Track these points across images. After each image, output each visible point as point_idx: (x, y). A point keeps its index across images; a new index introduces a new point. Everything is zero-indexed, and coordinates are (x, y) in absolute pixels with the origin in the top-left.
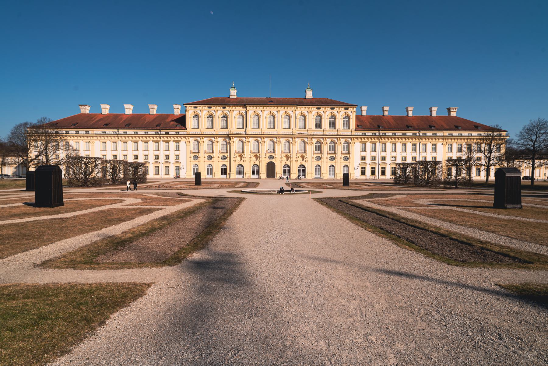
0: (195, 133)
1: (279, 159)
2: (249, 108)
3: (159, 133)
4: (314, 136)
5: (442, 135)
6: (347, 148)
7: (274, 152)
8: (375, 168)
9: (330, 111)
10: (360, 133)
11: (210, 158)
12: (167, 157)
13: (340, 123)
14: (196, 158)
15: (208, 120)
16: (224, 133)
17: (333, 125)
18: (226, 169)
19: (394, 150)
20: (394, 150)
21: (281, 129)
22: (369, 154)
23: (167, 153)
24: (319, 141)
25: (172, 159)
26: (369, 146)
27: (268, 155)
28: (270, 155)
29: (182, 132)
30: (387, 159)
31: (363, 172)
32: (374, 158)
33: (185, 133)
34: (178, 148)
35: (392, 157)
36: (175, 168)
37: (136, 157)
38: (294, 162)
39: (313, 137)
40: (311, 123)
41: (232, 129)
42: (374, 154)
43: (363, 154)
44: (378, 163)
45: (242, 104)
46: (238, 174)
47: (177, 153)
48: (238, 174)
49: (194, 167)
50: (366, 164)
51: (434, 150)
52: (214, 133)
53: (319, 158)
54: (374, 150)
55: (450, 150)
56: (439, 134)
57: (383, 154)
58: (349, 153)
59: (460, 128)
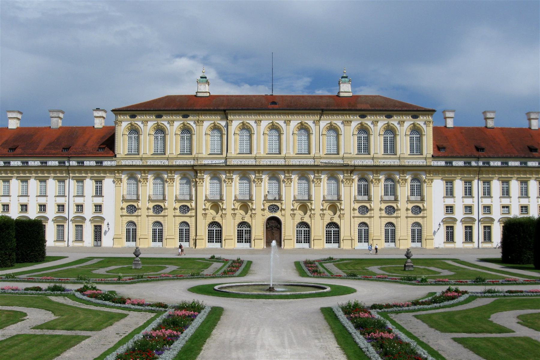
1: (288, 212)
7: (280, 200)
8: (471, 228)
9: (384, 120)
12: (80, 207)
14: (132, 209)
15: (156, 138)
18: (188, 231)
20: (506, 193)
21: (292, 154)
23: (79, 200)
25: (89, 212)
26: (459, 185)
27: (267, 205)
28: (271, 204)
31: (450, 237)
32: (469, 209)
33: (114, 163)
34: (99, 192)
35: (503, 207)
36: (93, 228)
37: (24, 207)
38: (318, 217)
41: (200, 156)
42: (468, 201)
43: (449, 201)
44: (477, 218)
46: (210, 240)
47: (98, 201)
48: (210, 240)
49: (128, 228)
50: (455, 220)
54: (468, 192)
57: (486, 201)
58: (422, 200)
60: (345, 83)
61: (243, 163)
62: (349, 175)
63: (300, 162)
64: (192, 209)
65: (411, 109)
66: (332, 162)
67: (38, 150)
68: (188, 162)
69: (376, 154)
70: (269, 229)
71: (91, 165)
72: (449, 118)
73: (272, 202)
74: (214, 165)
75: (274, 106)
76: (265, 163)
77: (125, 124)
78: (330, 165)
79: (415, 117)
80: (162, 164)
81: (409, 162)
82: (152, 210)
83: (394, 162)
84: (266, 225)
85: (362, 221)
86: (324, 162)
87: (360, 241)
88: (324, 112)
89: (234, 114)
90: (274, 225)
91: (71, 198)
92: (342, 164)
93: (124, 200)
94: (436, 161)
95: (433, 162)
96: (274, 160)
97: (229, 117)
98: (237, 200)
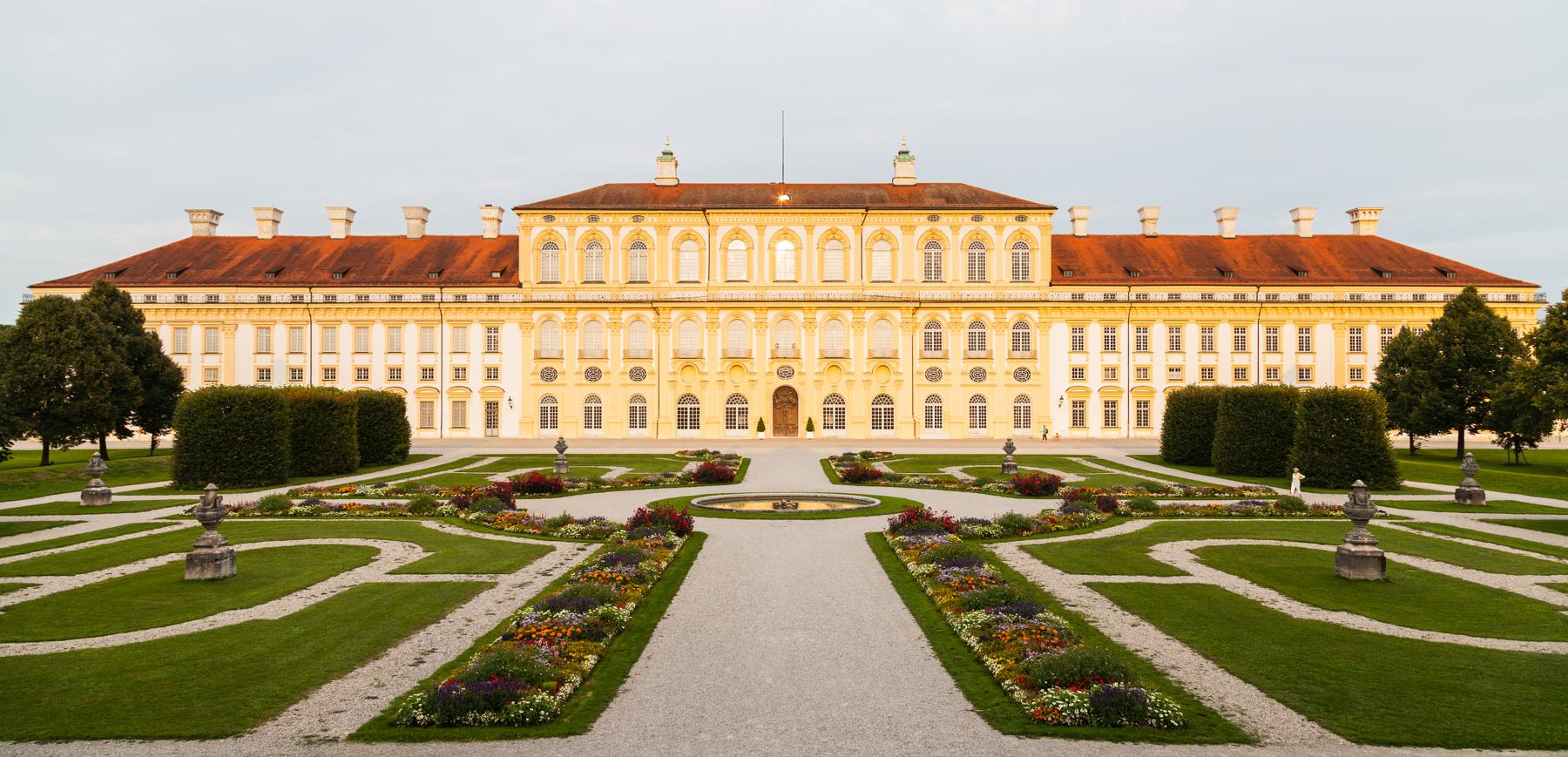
0: (547, 298)
2: (715, 217)
3: (437, 298)
4: (919, 304)
5: (1331, 298)
6: (1021, 341)
8: (1114, 404)
10: (1065, 292)
11: (593, 374)
12: (460, 373)
13: (999, 265)
14: (549, 375)
16: (638, 298)
17: (977, 270)
18: (643, 409)
19: (1176, 345)
20: (1176, 345)
22: (1094, 359)
23: (460, 360)
24: (938, 318)
25: (476, 379)
26: (1094, 336)
29: (506, 294)
30: (1122, 374)
31: (1078, 419)
32: (1111, 373)
34: (492, 346)
37: (363, 374)
39: (917, 308)
40: (913, 266)
41: (663, 285)
42: (1111, 359)
43: (1078, 360)
46: (682, 424)
47: (492, 360)
50: (1088, 391)
51: (1305, 346)
52: (608, 298)
53: (934, 375)
54: (1110, 344)
55: (1356, 345)
56: (1318, 293)
57: (1142, 359)
58: (1034, 358)
59: (1386, 275)
64: (653, 373)
65: (1016, 205)
67: (385, 277)
70: (779, 407)
77: (536, 231)
82: (584, 377)
84: (774, 400)
87: (928, 424)
88: (869, 212)
90: (785, 399)
91: (447, 357)
93: (538, 358)
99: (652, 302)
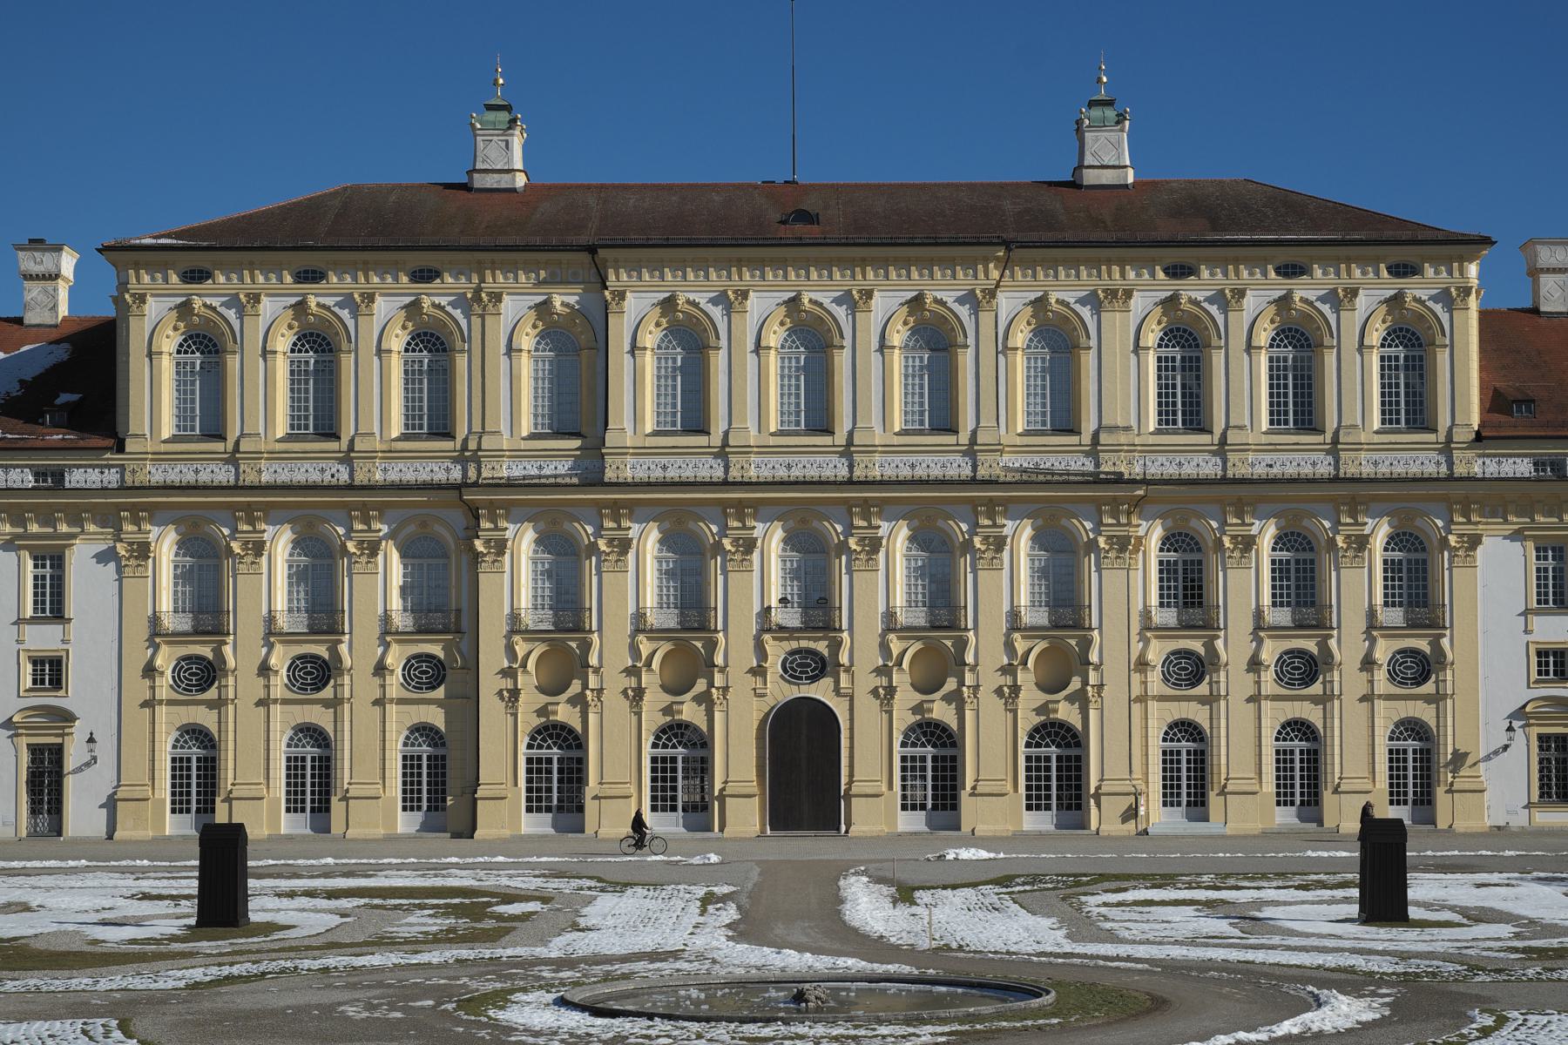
1: (866, 681)
28: (794, 645)
45: (572, 239)
47: (45, 638)
60: (1101, 125)
61: (672, 474)
62: (1123, 520)
63: (913, 466)
66: (1048, 465)
68: (436, 469)
69: (1236, 431)
71: (10, 484)
72: (1548, 271)
73: (798, 639)
74: (552, 480)
75: (800, 229)
76: (766, 474)
78: (1041, 478)
79: (1402, 270)
80: (327, 478)
81: (1376, 464)
83: (1314, 464)
85: (1177, 717)
86: (1017, 465)
89: (635, 267)
92: (1091, 474)
94: (1495, 456)
95: (1480, 462)
96: (804, 459)
97: (612, 276)
98: (652, 631)
99: (463, 486)
